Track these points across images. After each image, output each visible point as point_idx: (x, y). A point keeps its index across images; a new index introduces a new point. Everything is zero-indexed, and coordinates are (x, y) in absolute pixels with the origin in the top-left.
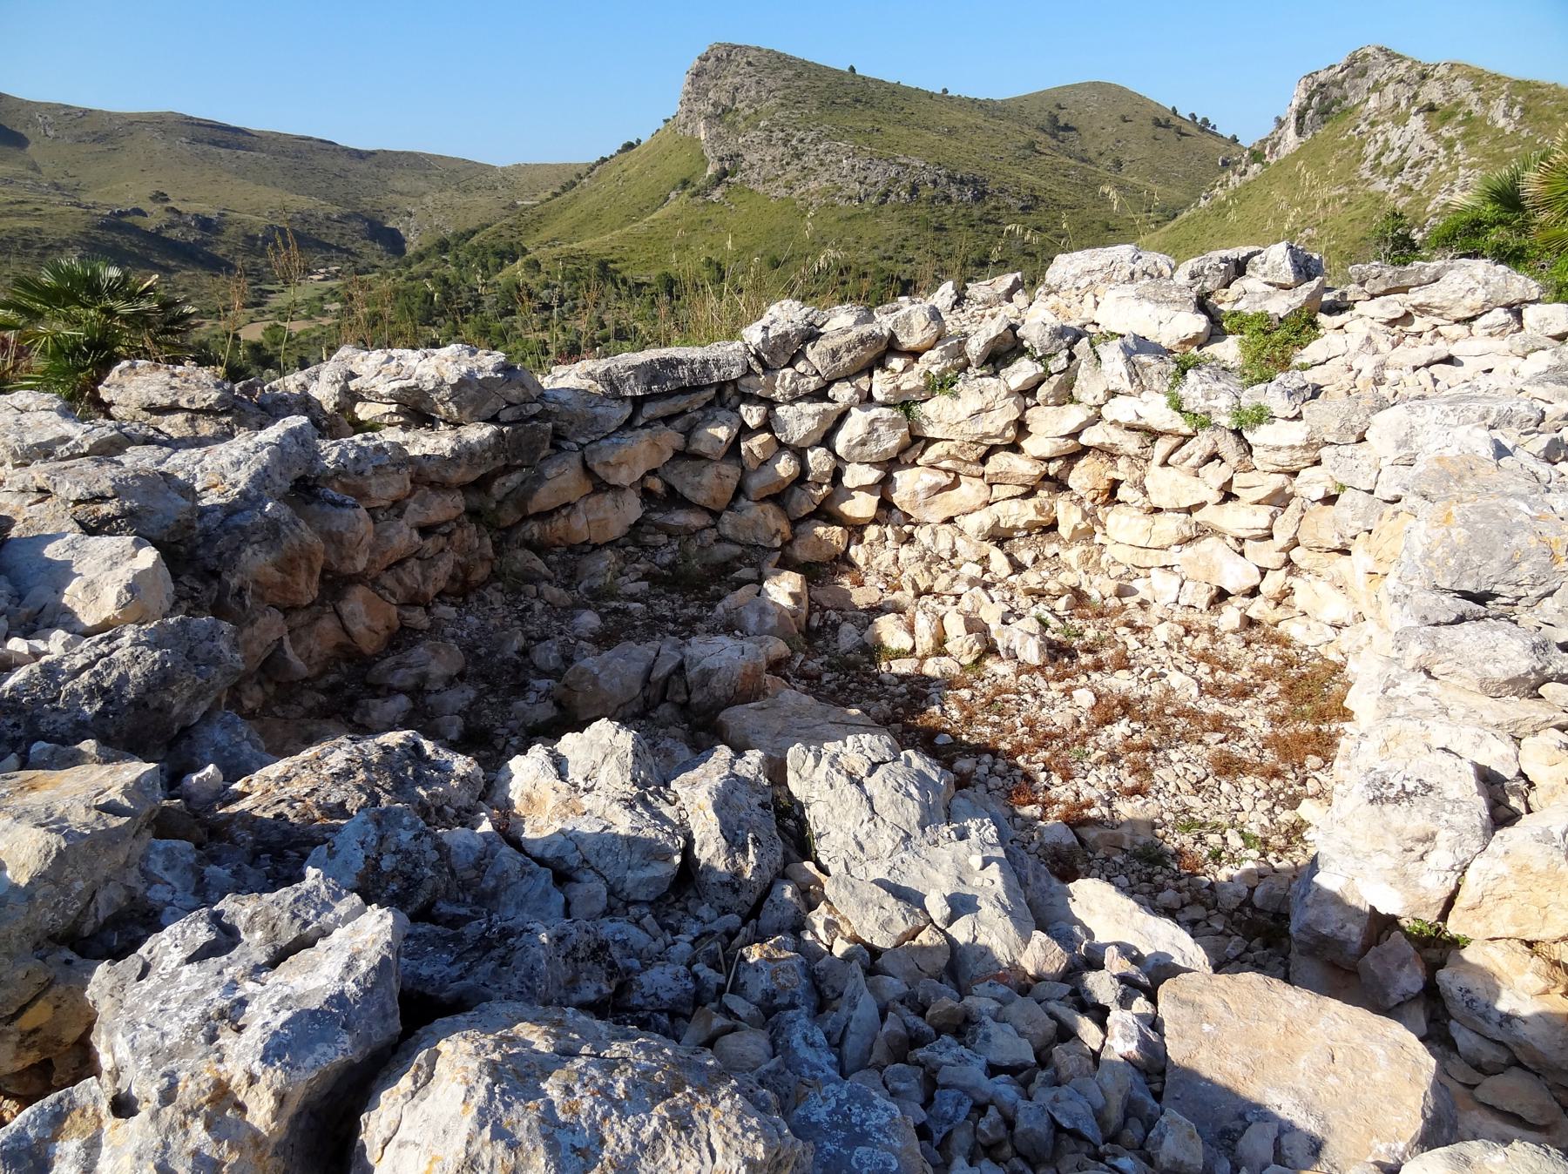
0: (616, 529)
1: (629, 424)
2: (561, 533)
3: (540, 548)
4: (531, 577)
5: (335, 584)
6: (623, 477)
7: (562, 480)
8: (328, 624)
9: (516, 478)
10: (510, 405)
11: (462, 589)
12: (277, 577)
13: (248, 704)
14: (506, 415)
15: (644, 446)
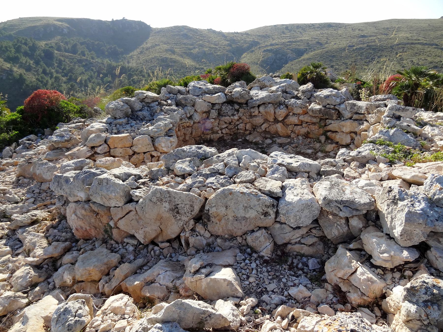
0: (344, 144)
1: (351, 118)
2: (333, 137)
3: (327, 138)
4: (320, 142)
5: (276, 121)
6: (344, 130)
7: (334, 125)
8: (274, 126)
9: (330, 121)
10: (328, 104)
11: (307, 136)
12: (265, 114)
13: (258, 130)
14: (328, 106)
15: (349, 124)
